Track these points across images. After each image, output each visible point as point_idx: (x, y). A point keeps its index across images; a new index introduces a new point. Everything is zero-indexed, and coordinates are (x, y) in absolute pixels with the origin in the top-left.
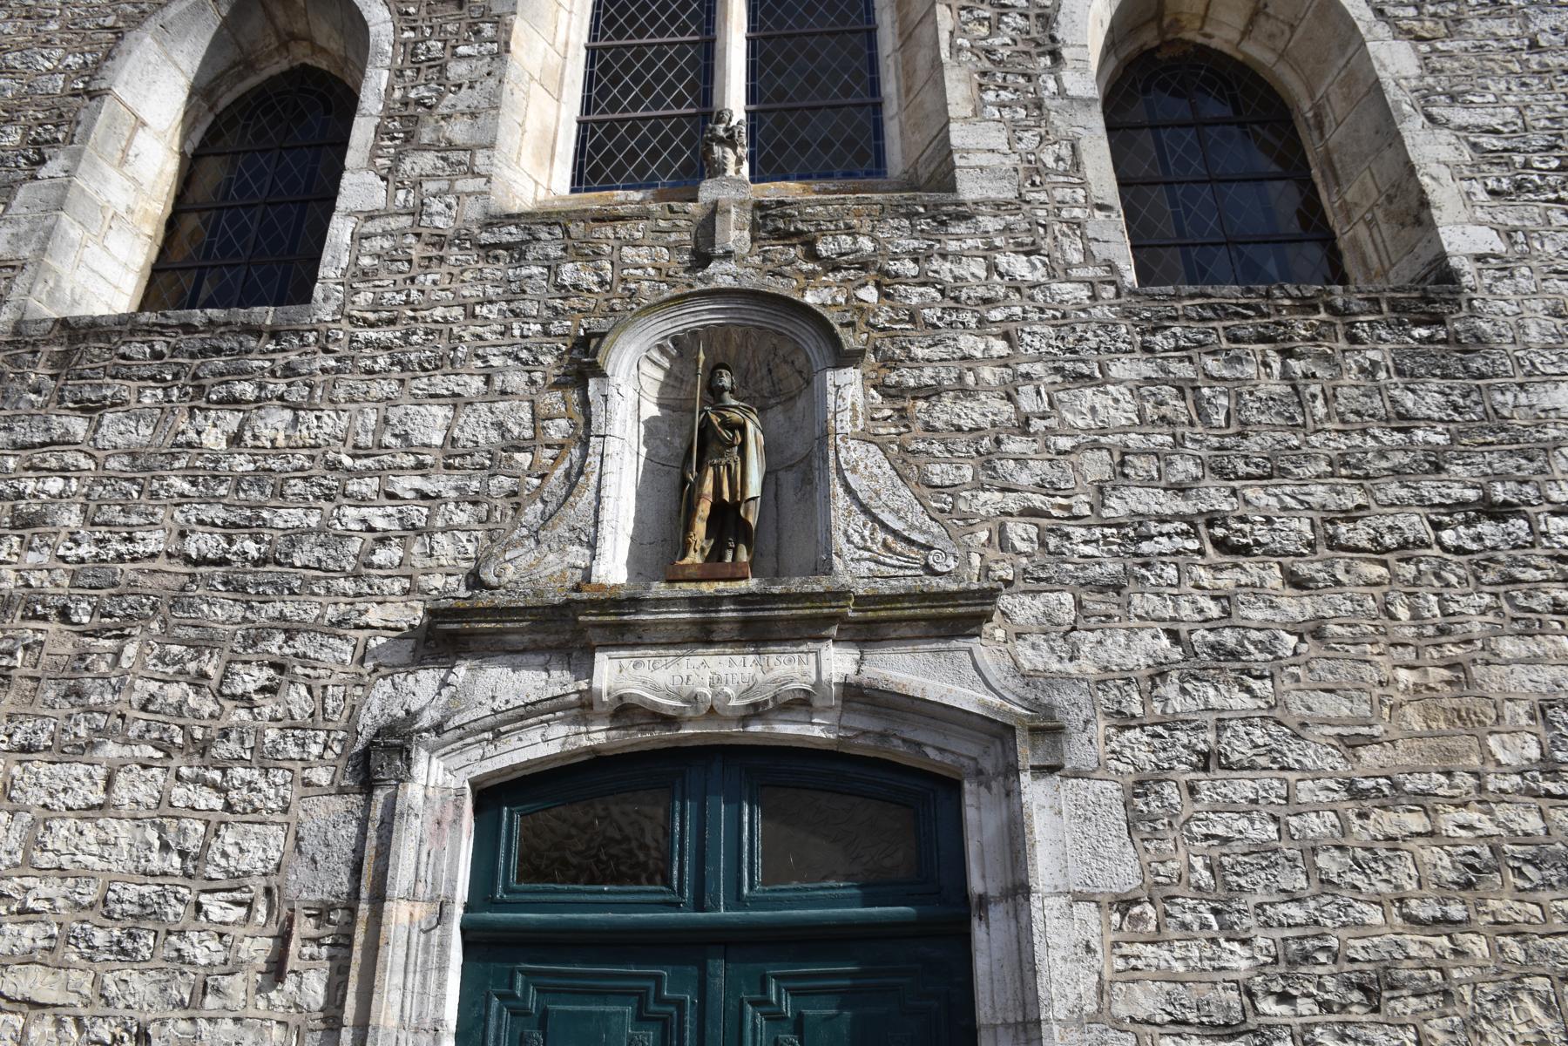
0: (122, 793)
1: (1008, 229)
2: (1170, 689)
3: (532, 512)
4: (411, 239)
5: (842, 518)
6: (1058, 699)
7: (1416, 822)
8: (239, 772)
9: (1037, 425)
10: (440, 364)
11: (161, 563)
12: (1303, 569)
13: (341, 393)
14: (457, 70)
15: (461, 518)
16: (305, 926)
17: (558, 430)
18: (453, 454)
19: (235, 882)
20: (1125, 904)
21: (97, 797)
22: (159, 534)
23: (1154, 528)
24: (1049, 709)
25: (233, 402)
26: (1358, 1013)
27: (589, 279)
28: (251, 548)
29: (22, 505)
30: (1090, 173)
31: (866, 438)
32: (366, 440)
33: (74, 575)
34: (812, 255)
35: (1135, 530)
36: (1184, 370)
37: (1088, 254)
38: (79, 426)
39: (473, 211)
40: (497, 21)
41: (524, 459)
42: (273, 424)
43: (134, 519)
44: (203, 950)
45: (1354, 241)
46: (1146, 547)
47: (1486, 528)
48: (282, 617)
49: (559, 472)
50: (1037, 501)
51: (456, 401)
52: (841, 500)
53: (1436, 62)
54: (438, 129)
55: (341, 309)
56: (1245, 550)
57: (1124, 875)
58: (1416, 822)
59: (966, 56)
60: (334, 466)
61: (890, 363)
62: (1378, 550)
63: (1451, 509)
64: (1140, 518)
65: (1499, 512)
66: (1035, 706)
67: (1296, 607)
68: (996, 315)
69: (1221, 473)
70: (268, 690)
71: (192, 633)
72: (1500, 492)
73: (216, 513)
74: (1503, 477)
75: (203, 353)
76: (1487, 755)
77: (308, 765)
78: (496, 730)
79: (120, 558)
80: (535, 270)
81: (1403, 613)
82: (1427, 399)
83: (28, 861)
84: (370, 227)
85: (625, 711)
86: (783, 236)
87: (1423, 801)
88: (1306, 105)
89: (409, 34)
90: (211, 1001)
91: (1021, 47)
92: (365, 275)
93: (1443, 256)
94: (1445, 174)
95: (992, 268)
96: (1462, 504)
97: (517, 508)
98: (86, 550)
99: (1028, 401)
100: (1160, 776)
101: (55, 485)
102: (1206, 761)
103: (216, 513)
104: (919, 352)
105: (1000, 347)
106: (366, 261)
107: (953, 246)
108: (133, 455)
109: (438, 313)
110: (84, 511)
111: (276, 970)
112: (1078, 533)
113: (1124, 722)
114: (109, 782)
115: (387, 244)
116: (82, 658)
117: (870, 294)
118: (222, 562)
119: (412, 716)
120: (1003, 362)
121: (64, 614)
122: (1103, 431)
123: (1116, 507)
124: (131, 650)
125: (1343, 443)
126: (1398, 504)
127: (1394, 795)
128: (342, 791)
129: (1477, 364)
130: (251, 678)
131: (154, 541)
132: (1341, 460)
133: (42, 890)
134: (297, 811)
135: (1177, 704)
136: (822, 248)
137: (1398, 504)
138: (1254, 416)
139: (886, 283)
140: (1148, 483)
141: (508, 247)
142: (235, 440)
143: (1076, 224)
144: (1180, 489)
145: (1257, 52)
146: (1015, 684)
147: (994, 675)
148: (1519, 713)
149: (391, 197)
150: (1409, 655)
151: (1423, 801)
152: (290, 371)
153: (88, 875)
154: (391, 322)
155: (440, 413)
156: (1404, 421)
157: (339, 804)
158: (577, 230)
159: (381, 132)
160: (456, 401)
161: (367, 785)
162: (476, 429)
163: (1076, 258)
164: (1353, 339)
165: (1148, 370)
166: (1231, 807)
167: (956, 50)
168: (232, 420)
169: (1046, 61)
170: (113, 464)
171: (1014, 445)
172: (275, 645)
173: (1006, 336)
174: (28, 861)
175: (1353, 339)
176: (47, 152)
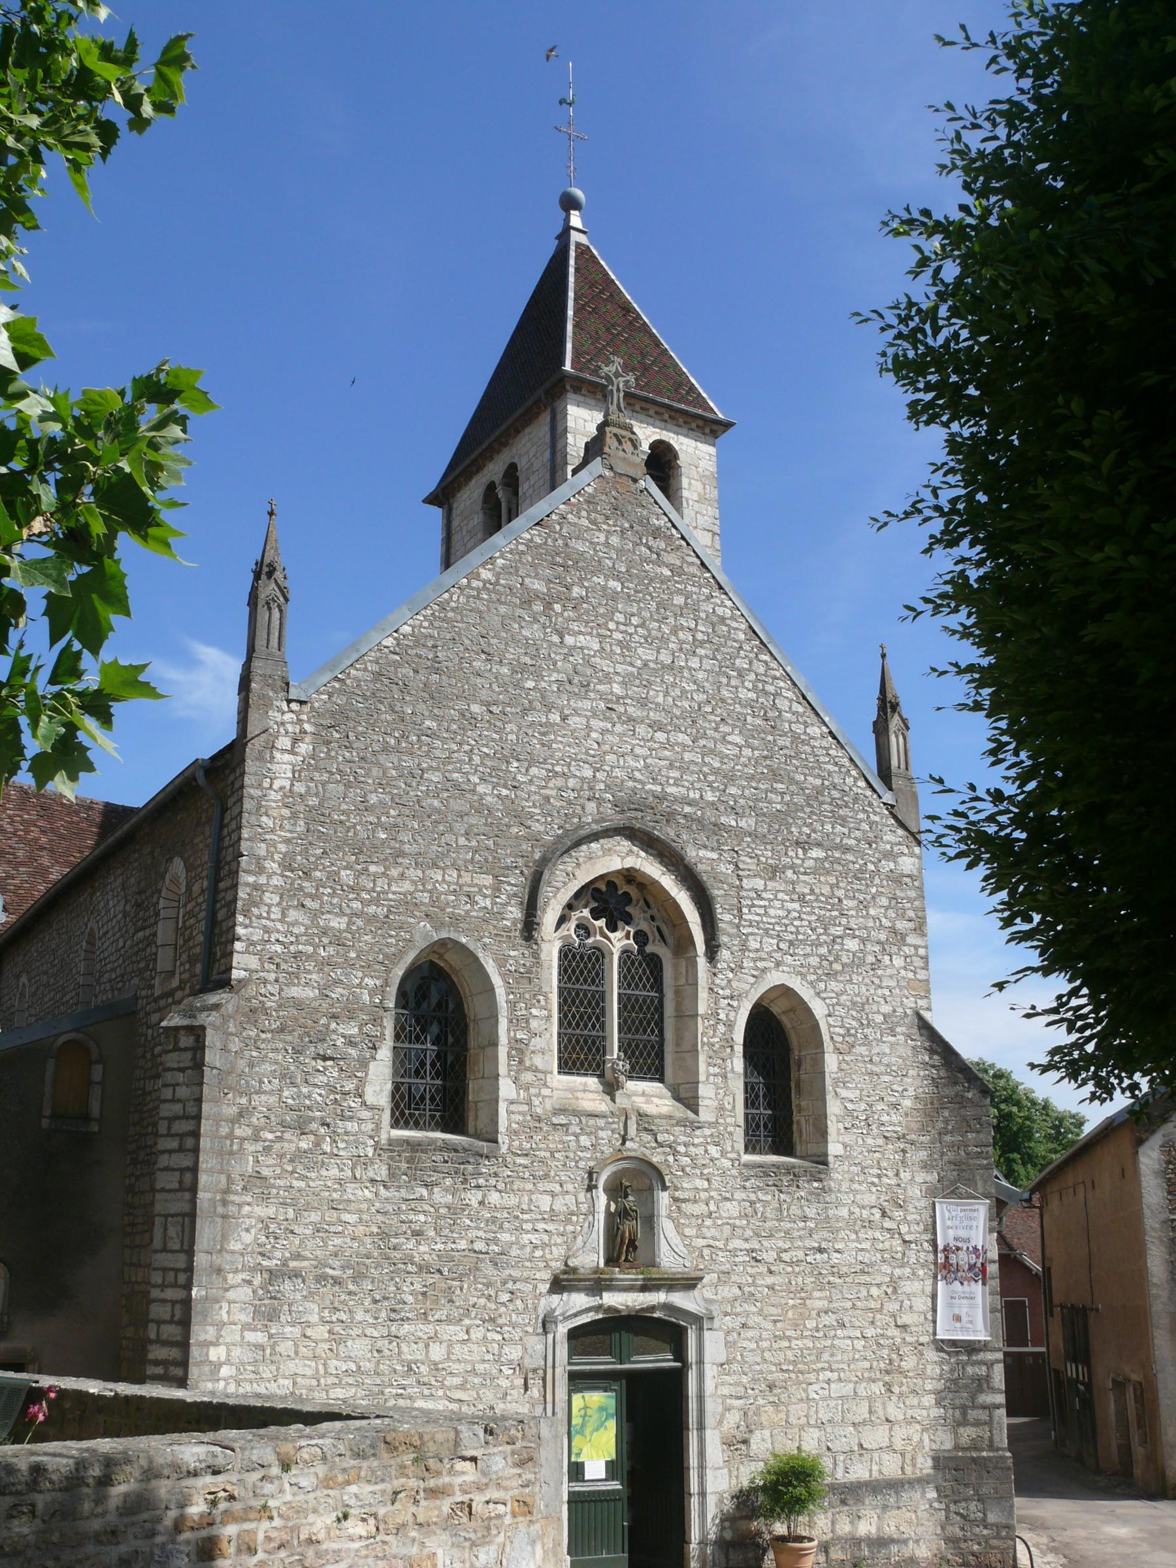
0: (473, 1336)
1: (712, 1135)
2: (737, 1304)
3: (580, 1239)
4: (529, 1118)
5: (664, 1248)
6: (712, 1308)
7: (786, 1344)
8: (506, 1328)
9: (714, 1215)
10: (546, 1176)
11: (466, 1253)
12: (773, 1268)
13: (515, 1187)
14: (534, 1024)
15: (559, 1241)
16: (530, 1375)
17: (584, 1208)
18: (553, 1215)
19: (510, 1362)
20: (722, 1365)
21: (466, 1337)
22: (464, 1242)
23: (739, 1253)
24: (710, 1311)
25: (478, 1187)
26: (767, 1393)
27: (588, 1144)
28: (496, 1249)
29: (413, 1226)
30: (737, 1111)
31: (669, 1217)
32: (525, 1207)
33: (438, 1256)
34: (656, 1141)
35: (734, 1252)
36: (753, 1197)
37: (732, 1147)
38: (424, 1192)
39: (548, 1105)
40: (547, 999)
41: (574, 1218)
42: (494, 1197)
43: (455, 1235)
44: (504, 1383)
45: (798, 1123)
46: (737, 1259)
47: (818, 1256)
48: (510, 1275)
49: (586, 1225)
50: (711, 1242)
51: (553, 1194)
52: (663, 1241)
53: (844, 1066)
54: (531, 1059)
55: (509, 1149)
56: (759, 1261)
57: (723, 1359)
58: (786, 1344)
59: (706, 1048)
60: (517, 1217)
61: (676, 1189)
62: (791, 1263)
63: (810, 1249)
64: (736, 1249)
65: (821, 1250)
66: (707, 1309)
67: (770, 1280)
68: (705, 1172)
69: (758, 1235)
70: (510, 1301)
71: (485, 1281)
72: (824, 1245)
73: (481, 1234)
74: (825, 1240)
75: (463, 1163)
76: (805, 1325)
77: (525, 1325)
78: (575, 1315)
79: (452, 1250)
80: (572, 1138)
81: (793, 1282)
82: (811, 1212)
83: (448, 1358)
84: (513, 1108)
85: (610, 1309)
86: (646, 1129)
87: (789, 1339)
88: (796, 1053)
89: (511, 996)
90: (509, 1398)
91: (723, 1043)
92: (516, 1132)
93: (826, 1155)
94: (834, 1119)
95: (706, 1151)
96: (814, 1248)
97: (575, 1238)
98: (439, 1246)
99: (713, 1207)
100: (734, 1330)
101: (422, 1218)
102: (744, 1326)
103: (481, 1234)
104: (685, 1185)
105: (706, 1185)
106: (514, 1126)
107: (696, 1141)
108: (449, 1208)
109: (542, 1154)
110: (435, 1229)
111: (526, 1387)
112: (721, 1254)
113: (726, 1314)
114: (468, 1332)
115: (521, 1118)
116: (450, 1288)
117: (671, 1159)
118: (487, 1253)
119: (554, 1310)
120: (706, 1190)
121: (439, 1271)
122: (730, 1218)
123: (731, 1246)
124: (466, 1286)
125: (789, 1225)
126: (799, 1248)
127: (785, 1337)
128: (538, 1334)
129: (828, 1199)
130: (505, 1297)
131: (463, 1245)
132: (787, 1232)
133: (455, 1367)
134: (525, 1339)
135: (739, 1309)
136: (660, 1138)
137: (799, 1248)
138: (768, 1215)
139: (675, 1153)
140: (739, 1238)
141: (561, 1125)
142: (481, 1203)
143: (731, 1134)
144: (746, 1240)
145: (785, 1020)
146: (702, 1303)
147: (699, 1300)
148: (814, 1313)
149: (518, 1094)
150: (792, 1295)
151: (789, 1339)
152: (496, 1175)
153: (466, 1361)
154: (526, 1155)
155: (548, 1198)
156: (805, 1219)
157: (536, 1338)
158: (583, 1119)
159: (509, 1056)
160: (553, 1194)
161: (545, 1332)
162: (559, 1205)
163: (729, 1149)
164: (798, 1187)
165: (744, 1196)
166: (747, 1339)
167: (703, 1044)
168: (479, 1195)
169: (729, 1050)
170: (443, 1211)
171: (708, 1222)
172: (510, 1285)
173: (708, 1180)
174: (448, 1358)
175: (798, 1187)
176: (377, 1044)
